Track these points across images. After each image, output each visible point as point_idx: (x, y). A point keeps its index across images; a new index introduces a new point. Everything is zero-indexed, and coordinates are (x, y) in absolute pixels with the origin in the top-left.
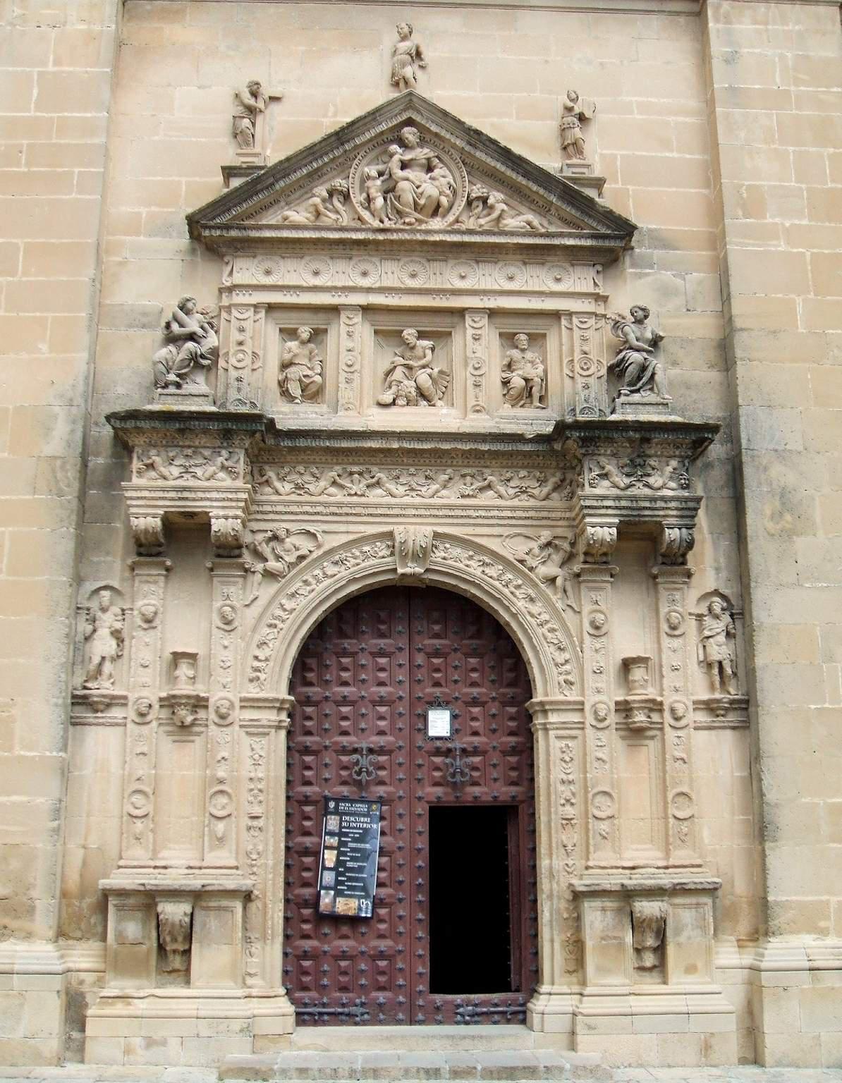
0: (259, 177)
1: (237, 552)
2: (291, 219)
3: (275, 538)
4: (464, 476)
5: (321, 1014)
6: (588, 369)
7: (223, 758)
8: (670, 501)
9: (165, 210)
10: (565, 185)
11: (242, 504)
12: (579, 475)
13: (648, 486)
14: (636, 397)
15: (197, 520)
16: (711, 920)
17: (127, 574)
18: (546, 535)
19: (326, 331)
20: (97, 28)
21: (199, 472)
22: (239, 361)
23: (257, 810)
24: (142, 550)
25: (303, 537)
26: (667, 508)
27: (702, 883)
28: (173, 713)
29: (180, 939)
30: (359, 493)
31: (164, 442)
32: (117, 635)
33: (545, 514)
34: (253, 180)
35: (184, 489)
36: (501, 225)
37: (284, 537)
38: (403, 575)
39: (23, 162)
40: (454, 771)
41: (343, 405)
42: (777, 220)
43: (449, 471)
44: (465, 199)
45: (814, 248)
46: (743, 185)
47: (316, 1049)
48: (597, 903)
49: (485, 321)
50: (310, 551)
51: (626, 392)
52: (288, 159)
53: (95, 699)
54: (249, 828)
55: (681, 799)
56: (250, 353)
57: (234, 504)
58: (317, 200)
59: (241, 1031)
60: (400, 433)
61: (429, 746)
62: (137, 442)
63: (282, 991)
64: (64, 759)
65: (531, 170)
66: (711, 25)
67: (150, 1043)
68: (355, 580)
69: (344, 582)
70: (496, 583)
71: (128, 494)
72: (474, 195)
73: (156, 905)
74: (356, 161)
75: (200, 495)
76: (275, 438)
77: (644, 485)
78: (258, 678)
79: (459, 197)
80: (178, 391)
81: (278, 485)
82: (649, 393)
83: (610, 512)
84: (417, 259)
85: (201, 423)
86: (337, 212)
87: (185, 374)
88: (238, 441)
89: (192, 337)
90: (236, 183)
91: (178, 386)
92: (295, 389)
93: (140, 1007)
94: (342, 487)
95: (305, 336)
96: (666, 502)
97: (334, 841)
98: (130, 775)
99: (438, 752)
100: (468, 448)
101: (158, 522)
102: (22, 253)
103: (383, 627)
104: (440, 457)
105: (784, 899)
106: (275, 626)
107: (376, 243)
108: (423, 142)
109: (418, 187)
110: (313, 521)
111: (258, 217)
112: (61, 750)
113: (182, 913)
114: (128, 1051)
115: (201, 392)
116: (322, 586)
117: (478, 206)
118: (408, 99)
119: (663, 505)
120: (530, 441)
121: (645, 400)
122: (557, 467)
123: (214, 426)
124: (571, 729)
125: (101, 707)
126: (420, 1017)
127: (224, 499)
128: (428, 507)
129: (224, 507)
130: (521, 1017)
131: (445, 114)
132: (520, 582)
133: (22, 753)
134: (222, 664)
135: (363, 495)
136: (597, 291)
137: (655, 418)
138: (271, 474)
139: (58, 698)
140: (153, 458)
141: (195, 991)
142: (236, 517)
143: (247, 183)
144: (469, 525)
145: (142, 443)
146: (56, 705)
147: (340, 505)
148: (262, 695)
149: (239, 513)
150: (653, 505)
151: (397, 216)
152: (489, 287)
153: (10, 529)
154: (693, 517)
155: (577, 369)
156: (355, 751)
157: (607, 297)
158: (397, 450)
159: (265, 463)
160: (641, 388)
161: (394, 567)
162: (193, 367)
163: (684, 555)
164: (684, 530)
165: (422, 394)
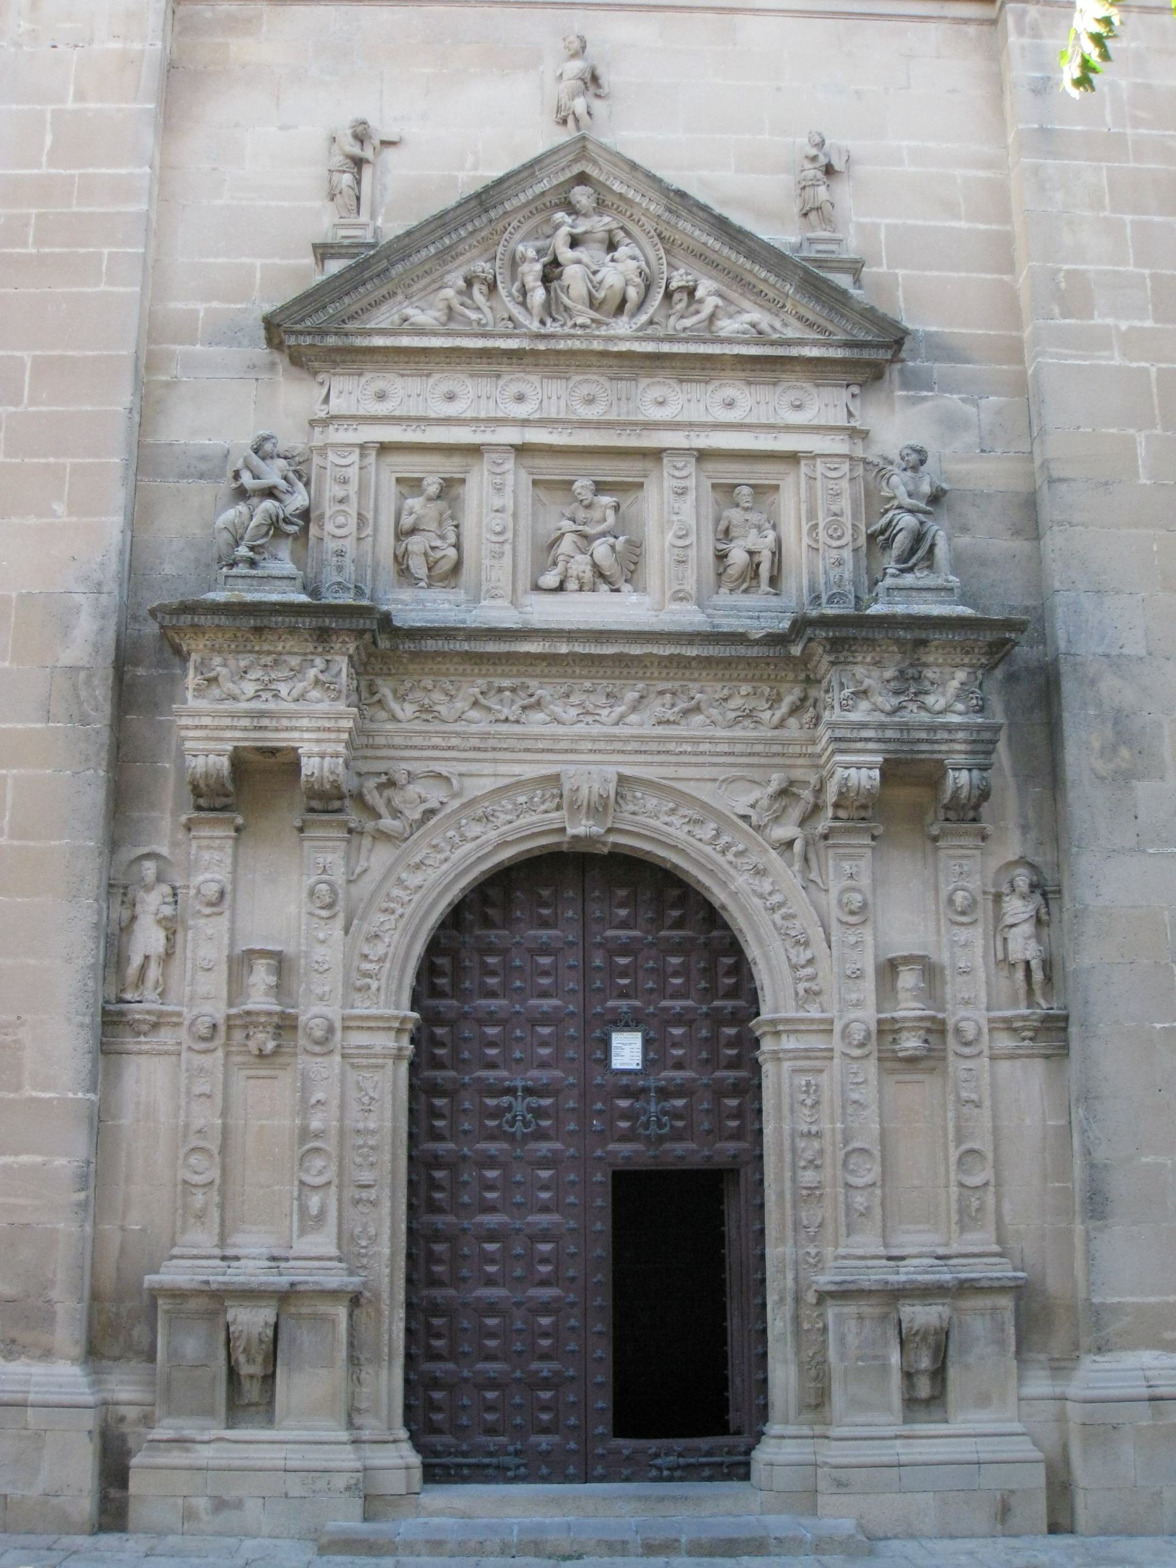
0: (367, 260)
1: (336, 804)
2: (412, 320)
3: (392, 784)
4: (661, 693)
5: (460, 1466)
6: (839, 538)
7: (318, 1101)
8: (957, 730)
9: (232, 306)
10: (806, 271)
11: (345, 736)
12: (827, 691)
13: (923, 707)
14: (909, 579)
15: (280, 758)
16: (1012, 1330)
17: (181, 835)
18: (776, 780)
19: (463, 481)
20: (137, 46)
21: (284, 689)
22: (339, 527)
23: (366, 1176)
24: (201, 801)
25: (431, 781)
26: (951, 741)
27: (998, 1279)
28: (248, 1037)
29: (260, 1359)
30: (511, 718)
31: (233, 646)
33: (776, 749)
34: (358, 265)
35: (262, 714)
36: (714, 328)
37: (404, 782)
38: (575, 838)
39: (31, 239)
40: (648, 1121)
41: (488, 591)
42: (1110, 321)
43: (641, 685)
44: (662, 291)
45: (1160, 361)
46: (1060, 270)
47: (452, 1516)
48: (850, 1309)
49: (691, 468)
50: (441, 803)
51: (894, 571)
52: (408, 233)
53: (137, 1017)
54: (358, 1202)
55: (969, 1159)
56: (355, 515)
57: (333, 736)
58: (449, 293)
59: (348, 1488)
60: (570, 632)
62: (194, 647)
63: (403, 1434)
64: (92, 1102)
65: (757, 248)
66: (1012, 39)
67: (220, 1505)
68: (505, 844)
69: (490, 848)
70: (708, 849)
71: (184, 721)
72: (674, 285)
73: (225, 1311)
74: (506, 235)
75: (285, 723)
76: (390, 639)
77: (919, 707)
78: (369, 987)
79: (653, 289)
80: (253, 572)
81: (395, 706)
82: (926, 573)
83: (871, 746)
84: (595, 377)
85: (287, 619)
86: (478, 309)
87: (261, 546)
88: (338, 645)
89: (270, 493)
90: (335, 267)
91: (253, 563)
92: (418, 566)
93: (205, 1455)
95: (433, 489)
96: (950, 731)
98: (187, 1126)
99: (626, 1092)
100: (667, 653)
101: (225, 762)
102: (28, 373)
103: (545, 912)
104: (627, 666)
105: (1115, 1300)
106: (393, 912)
107: (534, 353)
108: (601, 206)
109: (595, 273)
110: (446, 759)
111: (365, 317)
112: (88, 1091)
113: (262, 1323)
114: (189, 1515)
115: (285, 573)
116: (459, 853)
117: (681, 300)
118: (580, 145)
119: (946, 736)
120: (757, 642)
121: (921, 583)
122: (796, 681)
123: (307, 622)
124: (817, 1058)
125: (145, 1028)
126: (600, 1470)
127: (319, 729)
128: (610, 739)
129: (318, 741)
130: (742, 1470)
131: (634, 166)
132: (741, 847)
133: (34, 1094)
134: (316, 966)
135: (518, 722)
136: (853, 424)
137: (936, 610)
138: (385, 690)
139: (84, 1015)
140: (219, 669)
141: (282, 1432)
142: (336, 755)
143: (350, 268)
144: (669, 764)
145: (201, 646)
146: (82, 1025)
147: (484, 736)
148: (373, 1011)
149: (341, 748)
150: (932, 736)
151: (565, 315)
152: (694, 418)
153: (14, 771)
154: (989, 753)
155: (822, 535)
156: (511, 1091)
157: (867, 433)
158: (567, 655)
159: (377, 675)
160: (915, 565)
161: (561, 825)
162: (273, 536)
163: (976, 807)
164: (975, 773)
165: (599, 573)
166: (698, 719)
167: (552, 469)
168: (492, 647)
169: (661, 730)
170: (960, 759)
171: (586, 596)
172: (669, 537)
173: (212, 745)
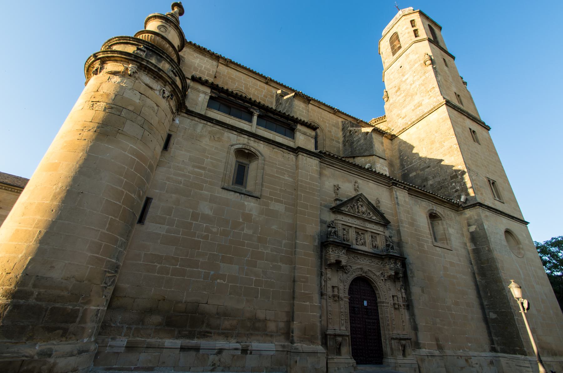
94: (354, 258)
107: (358, 217)
108: (361, 202)
131: (366, 198)
166: (373, 263)
167: (357, 230)
169: (369, 264)
171: (361, 246)
172: (369, 241)
173: (333, 259)
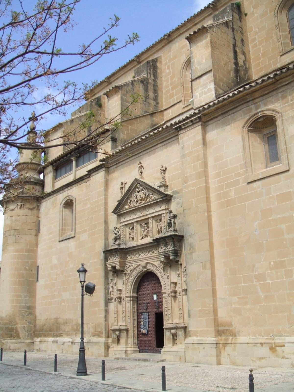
32: (112, 287)
35: (112, 262)
61: (154, 301)
97: (142, 320)
168: (133, 249)
170: (171, 255)
